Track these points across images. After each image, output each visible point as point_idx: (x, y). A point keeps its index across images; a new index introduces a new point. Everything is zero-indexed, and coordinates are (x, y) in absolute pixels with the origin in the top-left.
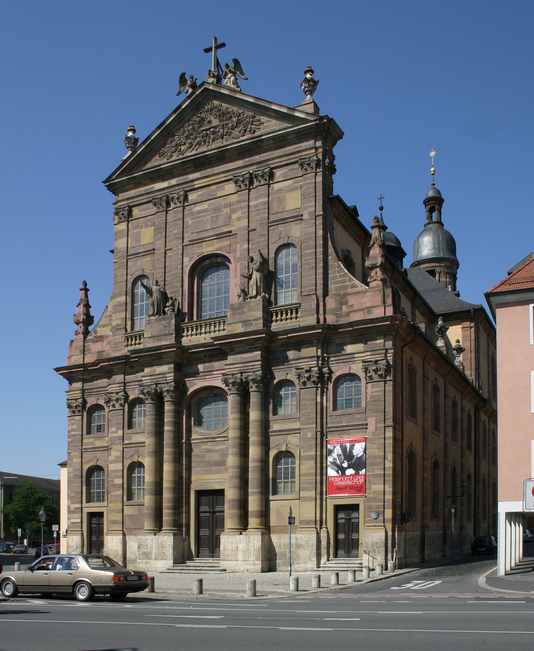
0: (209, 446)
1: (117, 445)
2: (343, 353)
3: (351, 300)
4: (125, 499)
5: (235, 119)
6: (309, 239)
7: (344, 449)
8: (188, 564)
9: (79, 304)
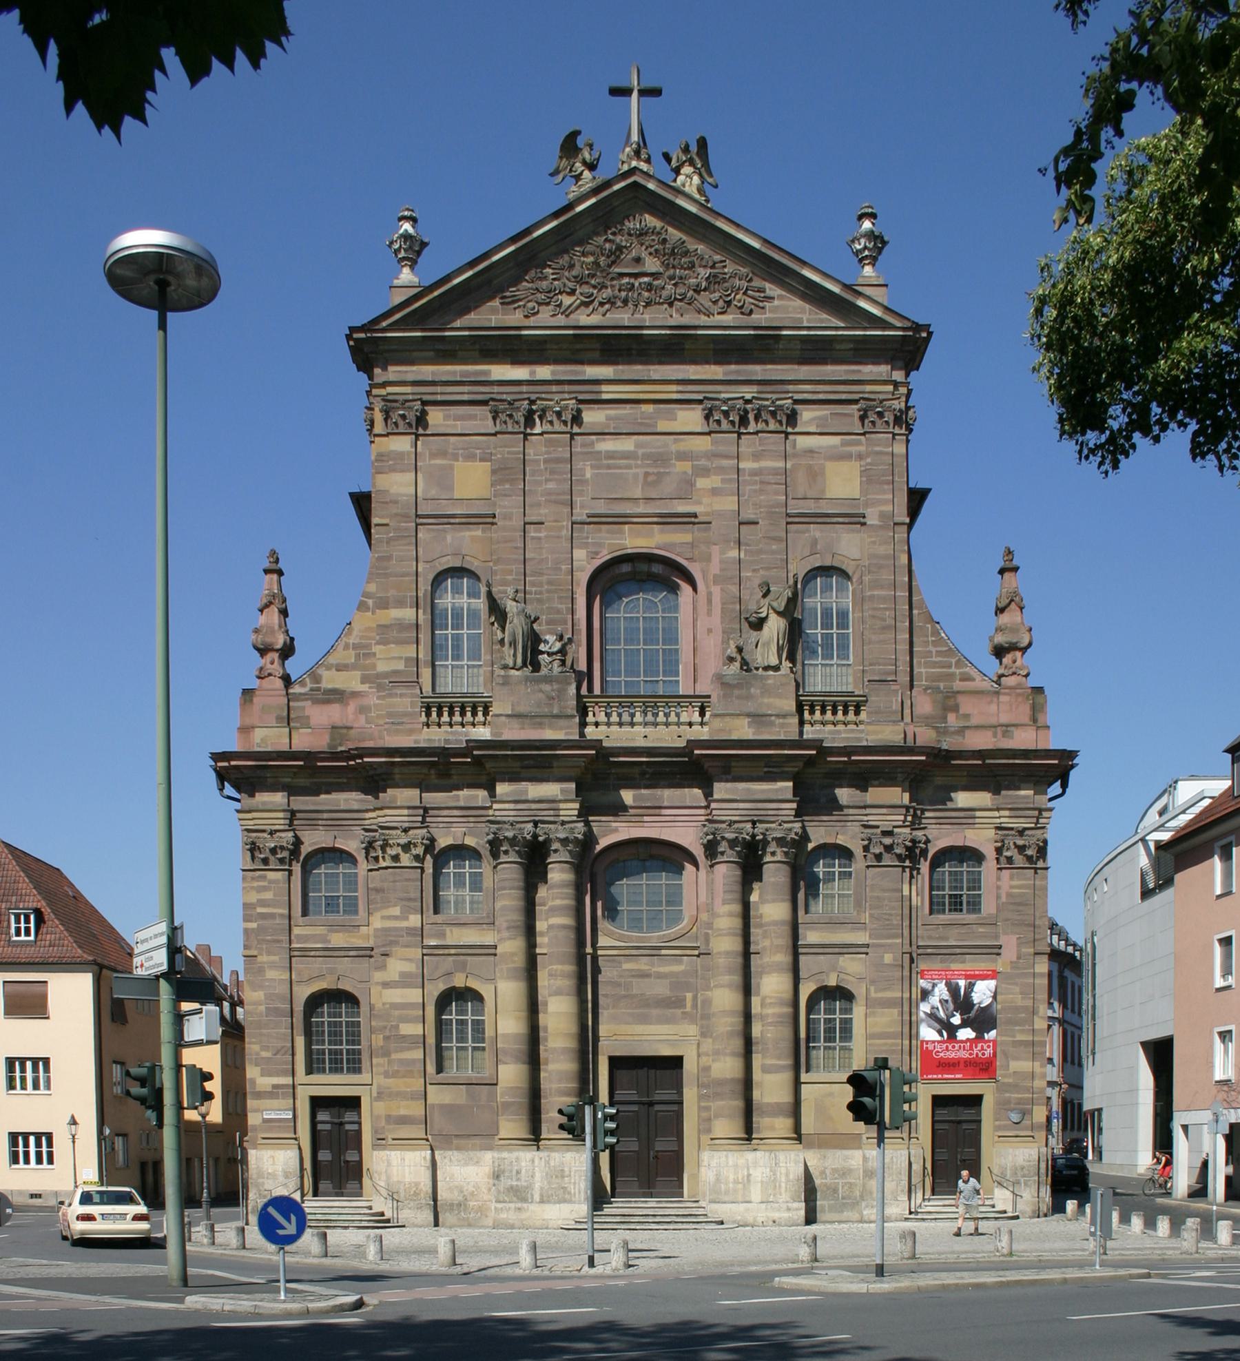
0: (642, 965)
1: (406, 946)
2: (950, 805)
3: (967, 705)
4: (431, 1068)
5: (704, 273)
6: (880, 567)
7: (953, 990)
8: (606, 1211)
9: (267, 606)
